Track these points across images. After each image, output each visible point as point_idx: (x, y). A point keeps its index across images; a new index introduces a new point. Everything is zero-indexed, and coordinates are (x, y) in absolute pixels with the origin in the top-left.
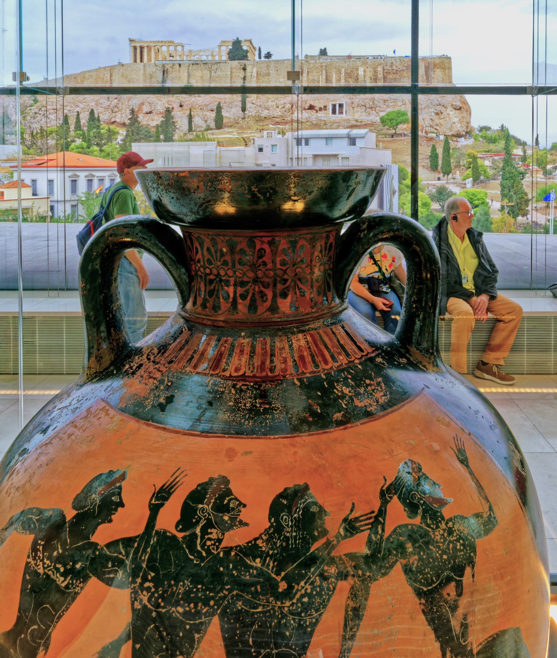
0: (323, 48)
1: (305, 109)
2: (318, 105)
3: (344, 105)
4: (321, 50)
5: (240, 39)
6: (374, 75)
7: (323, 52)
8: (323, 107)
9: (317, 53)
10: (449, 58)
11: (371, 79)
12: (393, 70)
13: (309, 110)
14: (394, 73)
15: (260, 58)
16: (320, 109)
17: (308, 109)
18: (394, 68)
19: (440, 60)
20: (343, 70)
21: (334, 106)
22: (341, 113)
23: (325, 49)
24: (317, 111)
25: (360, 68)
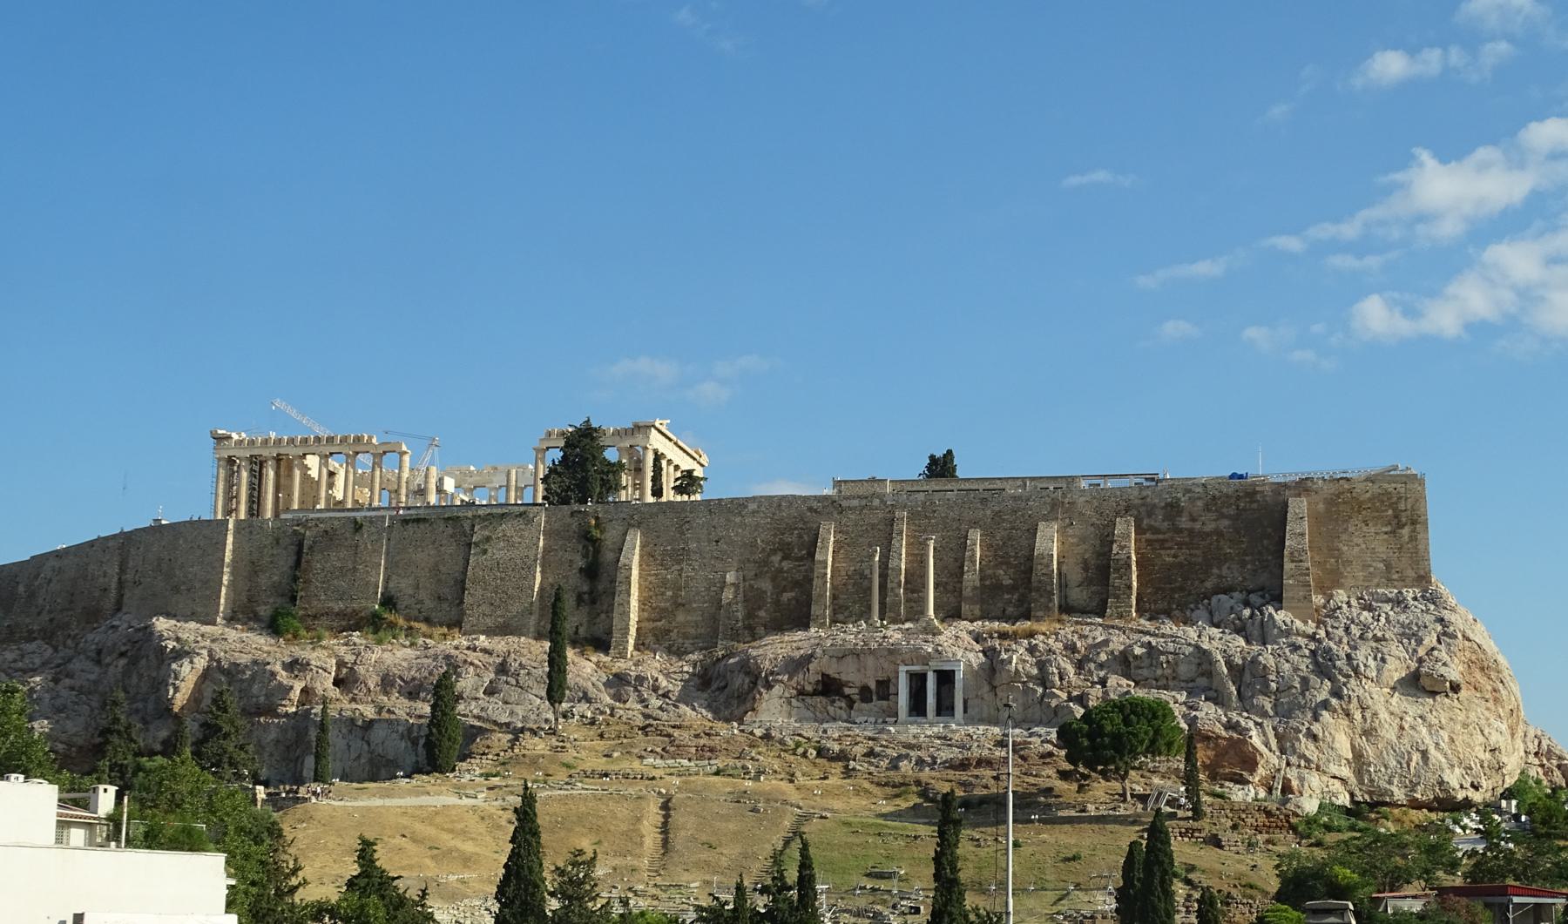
0: (939, 454)
1: (801, 693)
2: (850, 674)
3: (959, 676)
4: (932, 458)
5: (594, 425)
6: (1099, 555)
7: (941, 467)
8: (873, 686)
9: (915, 468)
10: (1413, 480)
11: (1086, 568)
12: (1179, 531)
13: (818, 699)
14: (1180, 545)
15: (657, 492)
16: (865, 694)
17: (815, 693)
18: (1184, 522)
19: (1374, 489)
20: (976, 536)
21: (918, 681)
22: (945, 708)
23: (950, 452)
24: (851, 703)
25: (1041, 525)
